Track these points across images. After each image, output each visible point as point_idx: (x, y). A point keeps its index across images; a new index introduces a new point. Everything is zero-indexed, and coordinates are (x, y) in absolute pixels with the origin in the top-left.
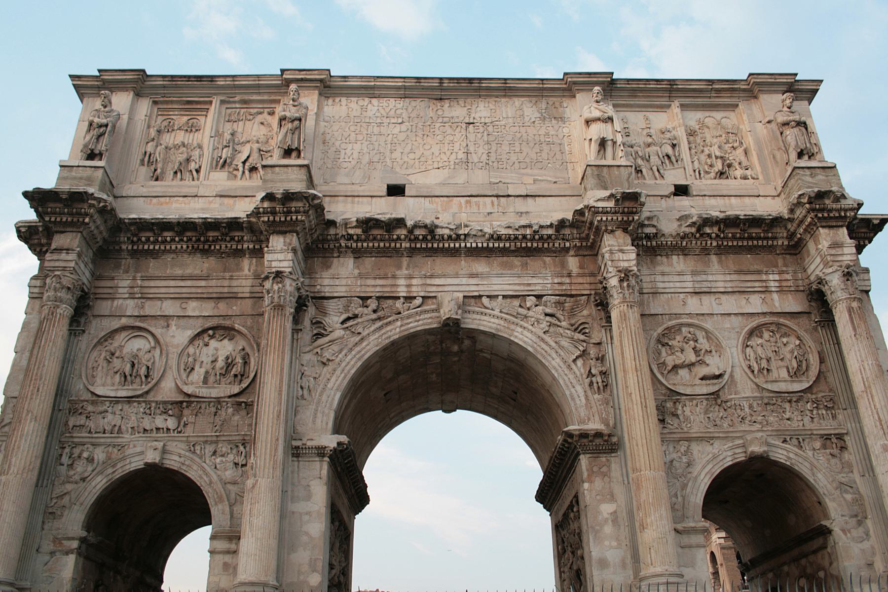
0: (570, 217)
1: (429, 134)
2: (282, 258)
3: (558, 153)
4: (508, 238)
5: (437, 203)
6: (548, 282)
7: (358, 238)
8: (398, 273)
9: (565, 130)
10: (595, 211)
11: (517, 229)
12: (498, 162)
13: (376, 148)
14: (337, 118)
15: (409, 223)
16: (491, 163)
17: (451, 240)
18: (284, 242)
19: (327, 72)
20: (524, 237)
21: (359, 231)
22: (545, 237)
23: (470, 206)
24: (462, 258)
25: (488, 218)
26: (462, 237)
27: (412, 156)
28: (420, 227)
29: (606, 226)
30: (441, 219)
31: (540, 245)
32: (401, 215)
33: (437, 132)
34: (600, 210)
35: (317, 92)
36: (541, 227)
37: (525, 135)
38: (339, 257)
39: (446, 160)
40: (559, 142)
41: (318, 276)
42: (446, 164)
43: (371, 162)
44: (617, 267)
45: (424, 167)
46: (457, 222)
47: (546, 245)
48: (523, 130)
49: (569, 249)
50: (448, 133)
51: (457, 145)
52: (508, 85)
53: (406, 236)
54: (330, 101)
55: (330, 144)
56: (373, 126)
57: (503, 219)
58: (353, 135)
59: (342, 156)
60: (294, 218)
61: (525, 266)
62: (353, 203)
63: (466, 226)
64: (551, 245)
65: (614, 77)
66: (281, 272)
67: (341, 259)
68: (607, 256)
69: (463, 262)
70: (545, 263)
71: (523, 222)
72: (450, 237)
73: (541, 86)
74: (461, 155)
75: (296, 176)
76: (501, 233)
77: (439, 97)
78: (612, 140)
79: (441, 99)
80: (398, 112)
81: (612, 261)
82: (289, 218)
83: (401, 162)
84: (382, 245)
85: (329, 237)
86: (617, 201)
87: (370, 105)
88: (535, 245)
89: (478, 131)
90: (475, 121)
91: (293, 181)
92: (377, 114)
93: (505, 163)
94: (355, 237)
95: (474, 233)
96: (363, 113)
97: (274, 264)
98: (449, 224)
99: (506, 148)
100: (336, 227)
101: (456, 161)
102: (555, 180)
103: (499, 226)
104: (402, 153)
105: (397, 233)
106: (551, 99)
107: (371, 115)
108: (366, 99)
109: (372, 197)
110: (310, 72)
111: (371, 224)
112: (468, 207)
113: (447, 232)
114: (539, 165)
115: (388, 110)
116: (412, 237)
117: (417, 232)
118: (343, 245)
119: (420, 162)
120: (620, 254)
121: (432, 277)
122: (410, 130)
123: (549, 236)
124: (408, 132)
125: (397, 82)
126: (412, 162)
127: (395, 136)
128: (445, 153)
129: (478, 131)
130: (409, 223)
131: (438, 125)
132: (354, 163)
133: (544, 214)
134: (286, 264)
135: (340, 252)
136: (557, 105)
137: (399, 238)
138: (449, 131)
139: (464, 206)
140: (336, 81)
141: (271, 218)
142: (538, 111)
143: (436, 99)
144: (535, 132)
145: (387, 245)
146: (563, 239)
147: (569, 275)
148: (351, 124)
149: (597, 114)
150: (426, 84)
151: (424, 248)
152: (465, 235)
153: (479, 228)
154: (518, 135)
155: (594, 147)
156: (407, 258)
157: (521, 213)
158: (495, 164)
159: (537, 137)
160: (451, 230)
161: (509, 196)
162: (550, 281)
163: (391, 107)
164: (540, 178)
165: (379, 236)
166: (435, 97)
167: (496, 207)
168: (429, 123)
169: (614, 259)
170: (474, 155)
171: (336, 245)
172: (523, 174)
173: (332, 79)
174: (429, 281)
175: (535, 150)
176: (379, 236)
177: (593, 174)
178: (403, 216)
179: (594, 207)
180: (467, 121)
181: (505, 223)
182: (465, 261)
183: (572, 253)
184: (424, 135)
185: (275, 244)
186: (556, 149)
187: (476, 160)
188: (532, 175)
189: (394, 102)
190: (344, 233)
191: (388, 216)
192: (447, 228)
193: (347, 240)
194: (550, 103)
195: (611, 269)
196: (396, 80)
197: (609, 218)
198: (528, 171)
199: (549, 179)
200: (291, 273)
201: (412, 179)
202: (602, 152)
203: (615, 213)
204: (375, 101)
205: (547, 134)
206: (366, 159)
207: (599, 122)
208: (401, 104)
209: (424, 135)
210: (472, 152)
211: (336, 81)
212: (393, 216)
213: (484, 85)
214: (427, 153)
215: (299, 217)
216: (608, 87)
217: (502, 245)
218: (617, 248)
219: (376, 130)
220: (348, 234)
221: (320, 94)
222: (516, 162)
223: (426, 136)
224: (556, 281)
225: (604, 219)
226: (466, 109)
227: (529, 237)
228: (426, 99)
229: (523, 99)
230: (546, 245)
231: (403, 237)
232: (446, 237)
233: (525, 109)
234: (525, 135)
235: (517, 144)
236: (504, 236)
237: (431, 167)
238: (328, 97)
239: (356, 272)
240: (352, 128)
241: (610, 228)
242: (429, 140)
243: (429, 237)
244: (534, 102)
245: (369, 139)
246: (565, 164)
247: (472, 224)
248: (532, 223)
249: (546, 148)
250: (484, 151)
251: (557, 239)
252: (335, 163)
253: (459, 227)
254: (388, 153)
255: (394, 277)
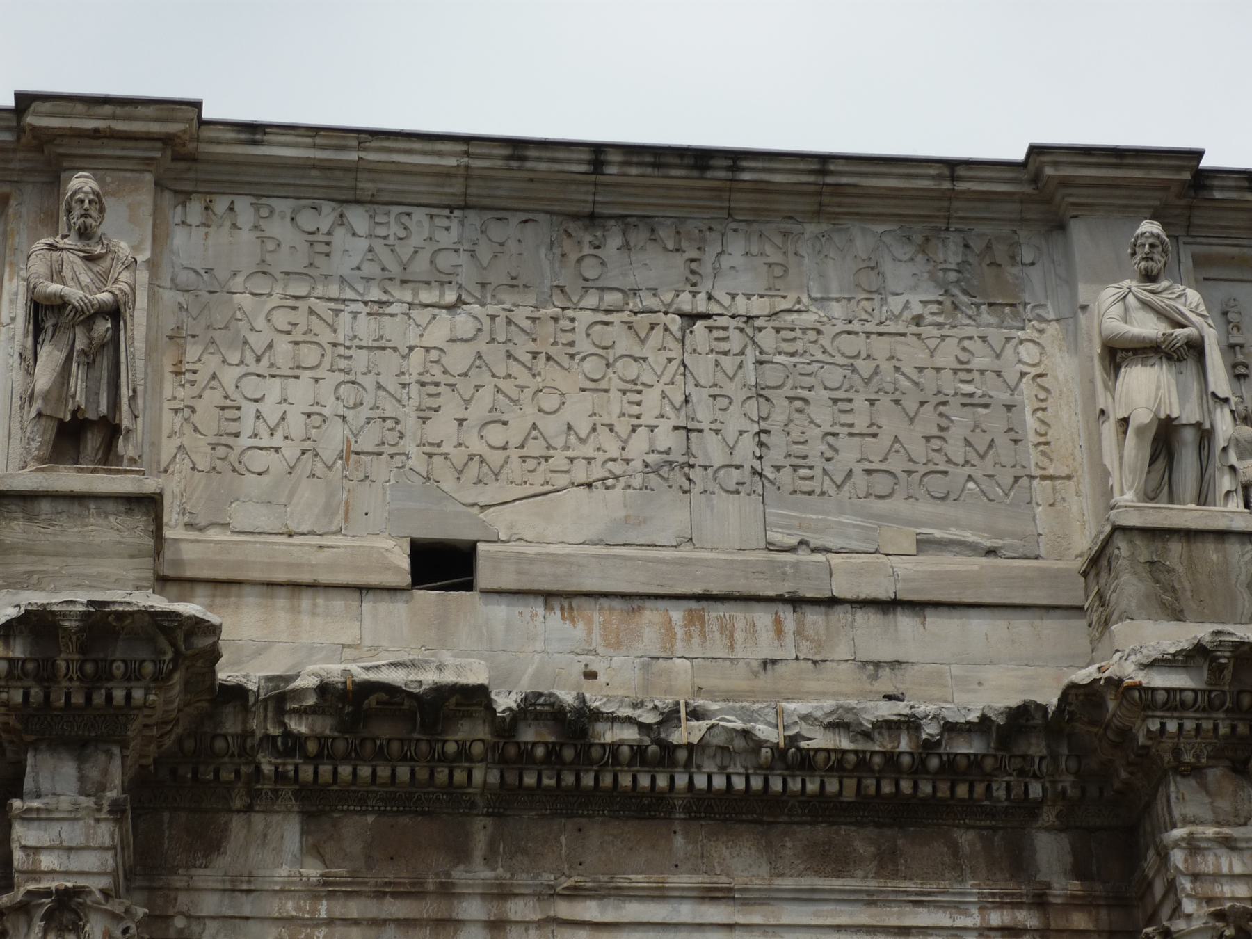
0: (1051, 699)
1: (553, 351)
2: (79, 840)
3: (1003, 441)
4: (836, 762)
5: (589, 622)
6: (969, 922)
7: (321, 748)
8: (458, 874)
9: (1028, 353)
10: (1144, 699)
11: (867, 735)
12: (795, 468)
13: (369, 400)
14: (222, 274)
15: (504, 702)
16: (769, 473)
17: (644, 763)
18: (82, 779)
19: (192, 113)
20: (891, 758)
21: (324, 725)
22: (963, 762)
23: (703, 635)
24: (677, 826)
25: (765, 681)
26: (682, 755)
27: (496, 435)
28: (538, 716)
29: (1176, 752)
30: (602, 679)
31: (944, 790)
32: (476, 676)
33: (584, 346)
34: (1161, 697)
35: (149, 177)
36: (950, 728)
37: (886, 367)
38: (248, 809)
39: (614, 451)
40: (1005, 397)
41: (178, 881)
42: (617, 468)
43: (348, 454)
44: (1210, 901)
45: (538, 478)
46: (665, 702)
47: (962, 791)
48: (881, 347)
49: (1039, 803)
50: (620, 349)
51: (651, 398)
52: (829, 180)
53: (490, 747)
54: (195, 209)
55: (202, 378)
56: (355, 314)
57: (813, 685)
58: (283, 346)
59: (247, 426)
60: (119, 695)
61: (887, 863)
62: (295, 610)
63: (695, 714)
64: (980, 789)
65: (1205, 163)
66: (78, 892)
67: (258, 820)
68: (1178, 858)
69: (679, 841)
70: (955, 849)
71: (887, 710)
72: (638, 752)
73: (946, 185)
74: (666, 438)
75: (111, 536)
76: (813, 744)
77: (588, 209)
78: (1198, 425)
79: (592, 219)
80: (445, 261)
81: (1196, 877)
82: (99, 698)
83: (459, 456)
84: (403, 772)
85: (220, 744)
86: (1216, 670)
87: (340, 233)
88: (926, 788)
89: (724, 346)
90: (715, 309)
91: (103, 554)
92: (370, 269)
93: (818, 472)
94: (312, 747)
95: (718, 739)
96: (320, 261)
97: (47, 861)
98: (635, 706)
99: (823, 415)
100: (246, 709)
101: (651, 459)
102: (989, 543)
103: (805, 718)
104: (461, 422)
105: (459, 736)
106: (979, 229)
107: (345, 271)
108: (327, 207)
109: (362, 590)
110: (128, 110)
111: (371, 701)
112: (696, 640)
113: (630, 734)
114: (937, 484)
115: (405, 252)
116: (512, 751)
117: (528, 735)
118: (267, 769)
119: (524, 458)
120: (1222, 852)
121: (575, 893)
122: (485, 336)
123: (975, 761)
124: (481, 345)
125: (440, 154)
126: (496, 458)
127: (434, 355)
128: (611, 428)
129: (724, 346)
130: (504, 702)
131: (585, 318)
132: (291, 452)
133: (955, 670)
134: (89, 861)
135: (254, 795)
136: (1000, 252)
137: (463, 753)
138: (625, 344)
139: (680, 632)
140: (219, 142)
141: (36, 693)
142: (932, 277)
143: (576, 217)
144: (922, 357)
145: (423, 774)
146: (1021, 773)
147: (1040, 902)
148: (275, 301)
149: (1148, 327)
150: (543, 166)
151: (548, 789)
152: (690, 747)
153: (739, 725)
154: (865, 368)
155: (1135, 450)
156: (488, 821)
157: (877, 665)
158: (785, 477)
159: (927, 380)
160: (644, 728)
161: (832, 602)
162: (973, 920)
163: (416, 240)
164: (938, 534)
165: (395, 746)
166: (574, 209)
167: (789, 639)
168: (551, 311)
169: (1202, 868)
170: (712, 441)
171: (244, 769)
172: (881, 517)
173: (207, 133)
174: (564, 909)
175: (921, 429)
176: (395, 746)
177: (1132, 558)
178: (486, 682)
179: (1138, 687)
180: (687, 308)
181: (829, 704)
182: (686, 834)
183: (1048, 816)
184: (535, 355)
185: (45, 786)
186: (995, 423)
187: (718, 459)
188: (910, 523)
189: (426, 222)
190: (273, 730)
191: (430, 677)
192: (631, 720)
193: (279, 754)
194: (978, 245)
195: (1189, 906)
196: (439, 146)
197: (1189, 725)
198: (897, 505)
199: (970, 537)
200: (105, 893)
201: (499, 521)
202: (1161, 464)
203: (1210, 707)
204: (358, 217)
205: (962, 369)
206: (334, 438)
207: (1155, 359)
208: (450, 232)
209: (535, 355)
210: (704, 426)
211: (219, 142)
212: (449, 678)
213: (746, 176)
214: (551, 426)
215: (138, 694)
216: (1179, 196)
217: (812, 786)
218: (1211, 831)
219: (366, 328)
220: (287, 734)
221: (159, 185)
222: (858, 469)
223: (542, 357)
224: (996, 919)
225: (1172, 727)
226: (679, 260)
227: (906, 760)
228: (540, 217)
229: (880, 228)
230: (962, 791)
231: (477, 749)
232: (625, 750)
233: (888, 267)
234: (886, 367)
235: (860, 403)
236: (821, 757)
237: (562, 480)
238: (188, 194)
239: (313, 872)
240: (281, 320)
241: (1188, 758)
242: (552, 374)
243: (568, 754)
244: (918, 239)
245: (342, 364)
246: (1024, 482)
247: (714, 706)
248: (922, 708)
249: (961, 419)
250: (745, 424)
251: (1000, 768)
252: (221, 451)
253: (670, 717)
254: (410, 422)
255: (447, 891)
